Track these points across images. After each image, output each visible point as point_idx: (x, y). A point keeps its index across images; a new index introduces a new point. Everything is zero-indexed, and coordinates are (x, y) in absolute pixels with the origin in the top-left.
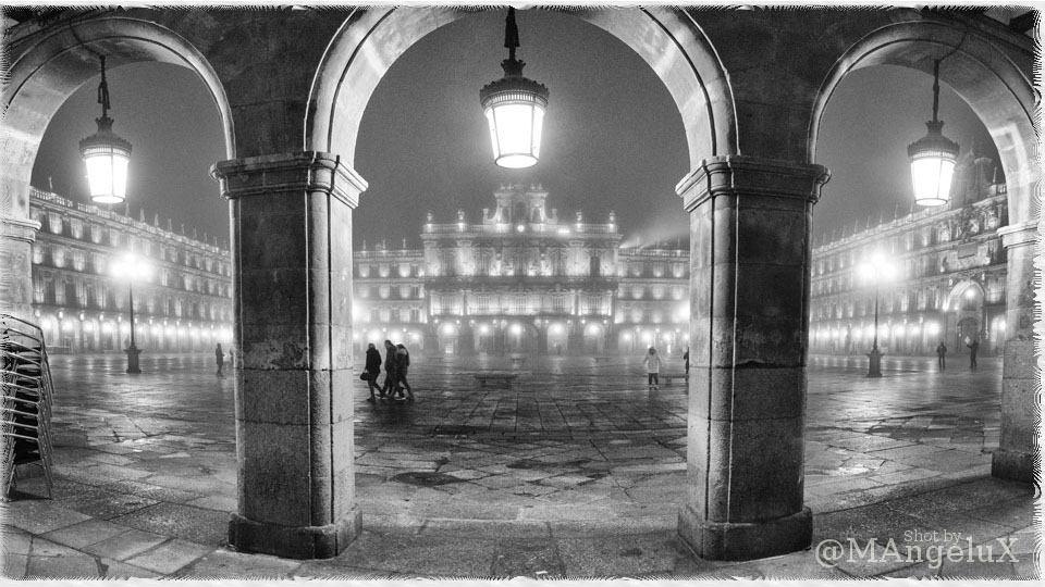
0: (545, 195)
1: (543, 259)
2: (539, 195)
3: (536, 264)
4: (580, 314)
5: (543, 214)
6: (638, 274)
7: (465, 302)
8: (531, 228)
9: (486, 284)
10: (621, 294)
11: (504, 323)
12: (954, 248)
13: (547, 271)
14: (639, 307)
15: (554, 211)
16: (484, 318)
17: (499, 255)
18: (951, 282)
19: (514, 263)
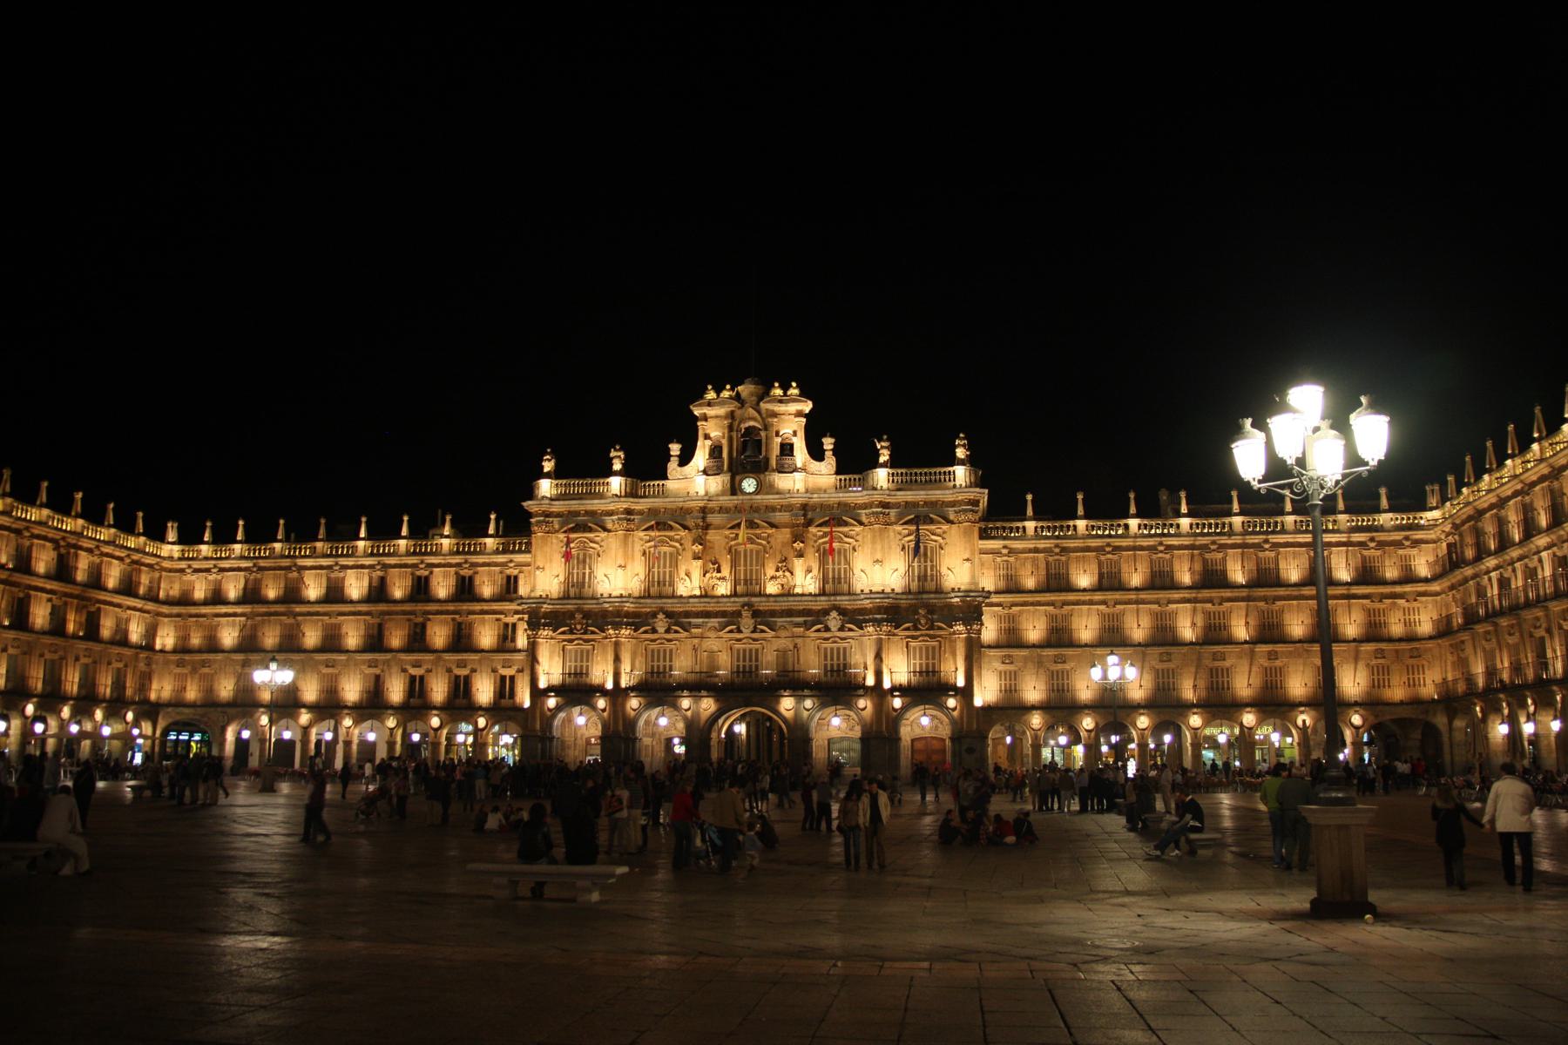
0: (807, 407)
1: (800, 555)
2: (793, 407)
3: (785, 566)
4: (887, 685)
5: (801, 454)
6: (1030, 583)
7: (617, 659)
8: (771, 489)
9: (669, 615)
10: (990, 631)
11: (708, 705)
13: (805, 581)
14: (1040, 663)
15: (828, 443)
16: (657, 690)
17: (698, 548)
19: (734, 564)
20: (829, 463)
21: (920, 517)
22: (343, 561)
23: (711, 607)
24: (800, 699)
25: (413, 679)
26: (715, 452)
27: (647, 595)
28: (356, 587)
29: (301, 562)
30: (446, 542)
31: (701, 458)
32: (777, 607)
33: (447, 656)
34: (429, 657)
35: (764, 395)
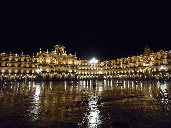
3: (63, 61)
4: (70, 72)
6: (80, 64)
7: (48, 69)
9: (53, 65)
11: (56, 73)
12: (144, 63)
15: (65, 51)
16: (52, 72)
18: (144, 68)
19: (58, 61)
20: (65, 53)
21: (73, 59)
22: (14, 56)
23: (57, 65)
24: (64, 73)
25: (24, 70)
26: (56, 51)
27: (50, 63)
28: (16, 60)
29: (8, 56)
30: (23, 55)
31: (55, 51)
32: (62, 65)
33: (29, 68)
34: (27, 68)
35: (61, 46)
